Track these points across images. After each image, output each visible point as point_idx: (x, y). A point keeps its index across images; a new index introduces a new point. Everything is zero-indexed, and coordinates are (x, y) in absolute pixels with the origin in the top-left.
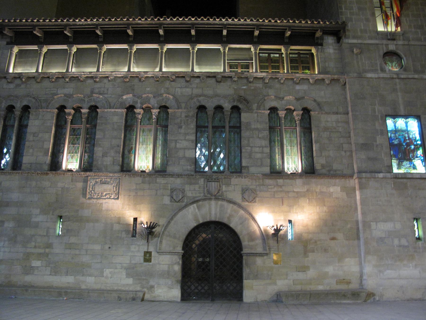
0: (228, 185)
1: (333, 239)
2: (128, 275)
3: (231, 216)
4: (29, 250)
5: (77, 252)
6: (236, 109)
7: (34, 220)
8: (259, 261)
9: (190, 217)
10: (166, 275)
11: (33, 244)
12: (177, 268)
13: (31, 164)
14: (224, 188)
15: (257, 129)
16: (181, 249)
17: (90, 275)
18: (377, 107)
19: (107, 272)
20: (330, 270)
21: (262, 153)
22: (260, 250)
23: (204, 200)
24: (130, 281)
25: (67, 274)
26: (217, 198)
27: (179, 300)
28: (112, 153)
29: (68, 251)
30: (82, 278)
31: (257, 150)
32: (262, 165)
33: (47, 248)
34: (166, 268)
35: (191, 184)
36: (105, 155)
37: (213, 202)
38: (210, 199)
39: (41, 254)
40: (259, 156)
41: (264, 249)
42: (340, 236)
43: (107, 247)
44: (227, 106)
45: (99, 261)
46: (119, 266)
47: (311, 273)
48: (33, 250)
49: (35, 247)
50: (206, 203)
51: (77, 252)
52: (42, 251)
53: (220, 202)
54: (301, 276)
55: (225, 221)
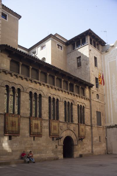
0: (71, 126)
1: (87, 141)
2: (52, 152)
3: (72, 135)
4: (26, 146)
5: (40, 146)
6: (71, 103)
7: (26, 135)
8: (76, 146)
9: (64, 135)
10: (60, 152)
11: (27, 144)
12: (62, 149)
13: (23, 113)
14: (70, 127)
15: (75, 110)
16: (63, 144)
17: (43, 153)
18: (95, 109)
19: (48, 152)
20: (87, 148)
21: (76, 117)
22: (77, 144)
23: (67, 130)
24: (53, 154)
25: (38, 153)
26: (70, 130)
27: (63, 158)
28: (46, 113)
29: (37, 146)
30: (42, 154)
31: (76, 116)
32: (77, 121)
33: (32, 145)
34: (60, 150)
35: (64, 125)
36: (45, 113)
37: (68, 131)
38: (68, 130)
39: (30, 147)
40: (76, 118)
41: (78, 143)
42: (88, 140)
43: (47, 144)
44: (70, 103)
45: (45, 148)
46: (50, 150)
47: (84, 149)
48: (27, 146)
49: (28, 145)
50: (67, 131)
51: (40, 146)
52: (29, 146)
53: (70, 131)
54: (83, 150)
55: (71, 136)
